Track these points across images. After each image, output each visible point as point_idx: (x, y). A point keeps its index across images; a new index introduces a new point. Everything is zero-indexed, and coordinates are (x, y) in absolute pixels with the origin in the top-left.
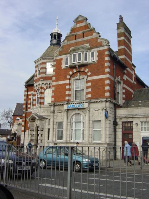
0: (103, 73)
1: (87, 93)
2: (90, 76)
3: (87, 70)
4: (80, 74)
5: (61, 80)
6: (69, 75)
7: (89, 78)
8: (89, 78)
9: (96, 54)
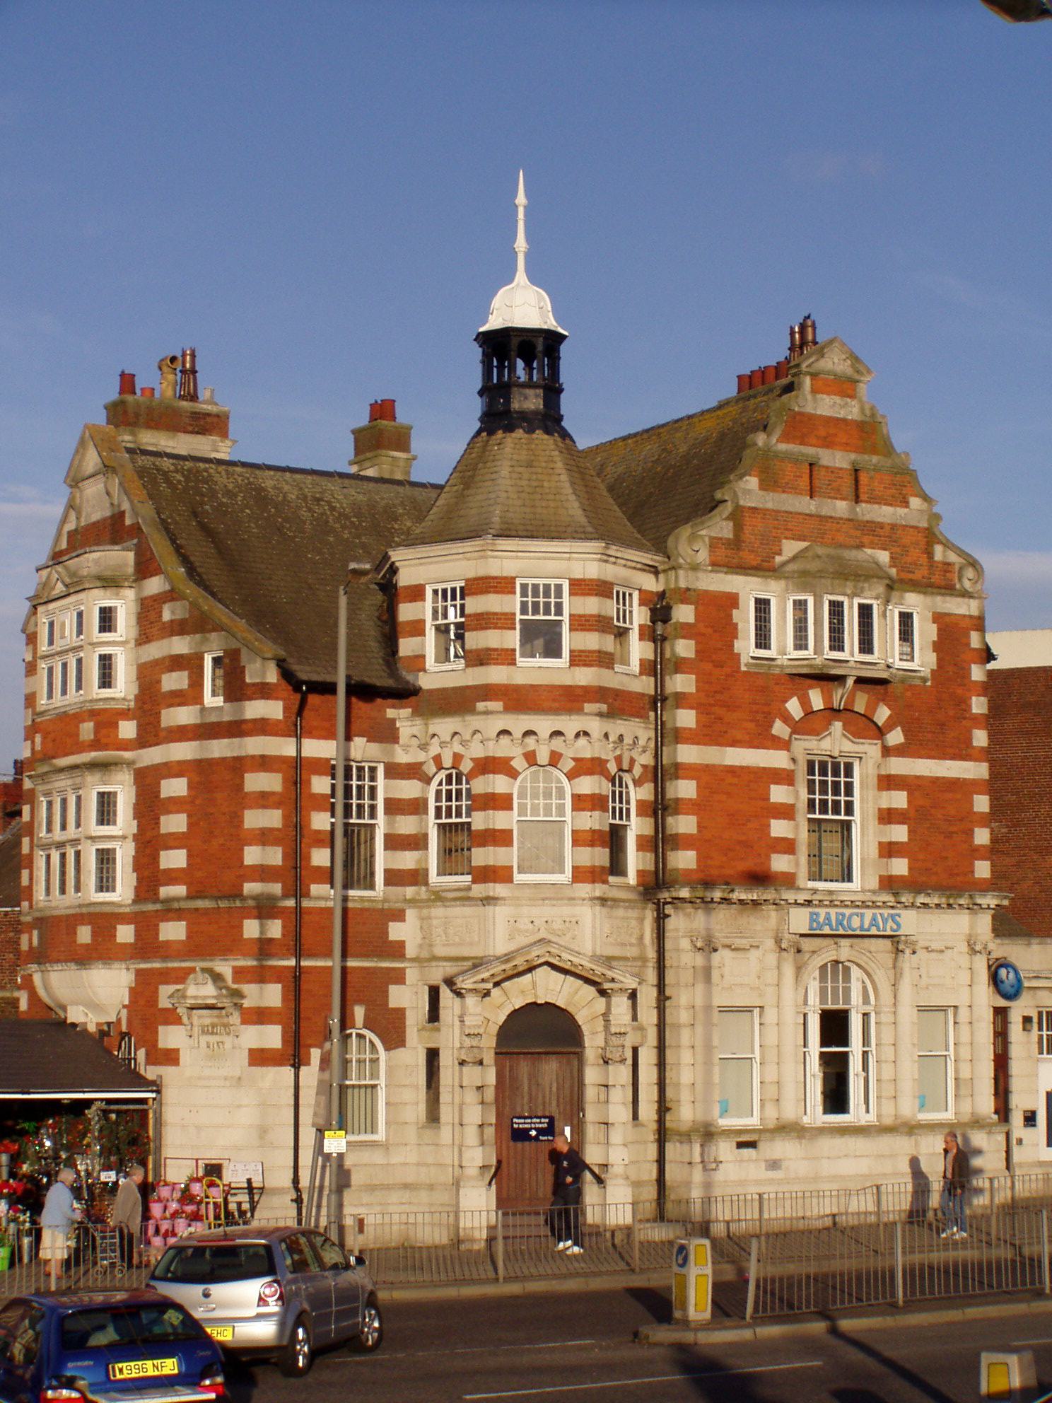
0: (963, 752)
1: (889, 850)
2: (900, 751)
3: (883, 714)
4: (845, 728)
5: (734, 743)
6: (787, 718)
7: (900, 766)
8: (900, 766)
9: (924, 631)
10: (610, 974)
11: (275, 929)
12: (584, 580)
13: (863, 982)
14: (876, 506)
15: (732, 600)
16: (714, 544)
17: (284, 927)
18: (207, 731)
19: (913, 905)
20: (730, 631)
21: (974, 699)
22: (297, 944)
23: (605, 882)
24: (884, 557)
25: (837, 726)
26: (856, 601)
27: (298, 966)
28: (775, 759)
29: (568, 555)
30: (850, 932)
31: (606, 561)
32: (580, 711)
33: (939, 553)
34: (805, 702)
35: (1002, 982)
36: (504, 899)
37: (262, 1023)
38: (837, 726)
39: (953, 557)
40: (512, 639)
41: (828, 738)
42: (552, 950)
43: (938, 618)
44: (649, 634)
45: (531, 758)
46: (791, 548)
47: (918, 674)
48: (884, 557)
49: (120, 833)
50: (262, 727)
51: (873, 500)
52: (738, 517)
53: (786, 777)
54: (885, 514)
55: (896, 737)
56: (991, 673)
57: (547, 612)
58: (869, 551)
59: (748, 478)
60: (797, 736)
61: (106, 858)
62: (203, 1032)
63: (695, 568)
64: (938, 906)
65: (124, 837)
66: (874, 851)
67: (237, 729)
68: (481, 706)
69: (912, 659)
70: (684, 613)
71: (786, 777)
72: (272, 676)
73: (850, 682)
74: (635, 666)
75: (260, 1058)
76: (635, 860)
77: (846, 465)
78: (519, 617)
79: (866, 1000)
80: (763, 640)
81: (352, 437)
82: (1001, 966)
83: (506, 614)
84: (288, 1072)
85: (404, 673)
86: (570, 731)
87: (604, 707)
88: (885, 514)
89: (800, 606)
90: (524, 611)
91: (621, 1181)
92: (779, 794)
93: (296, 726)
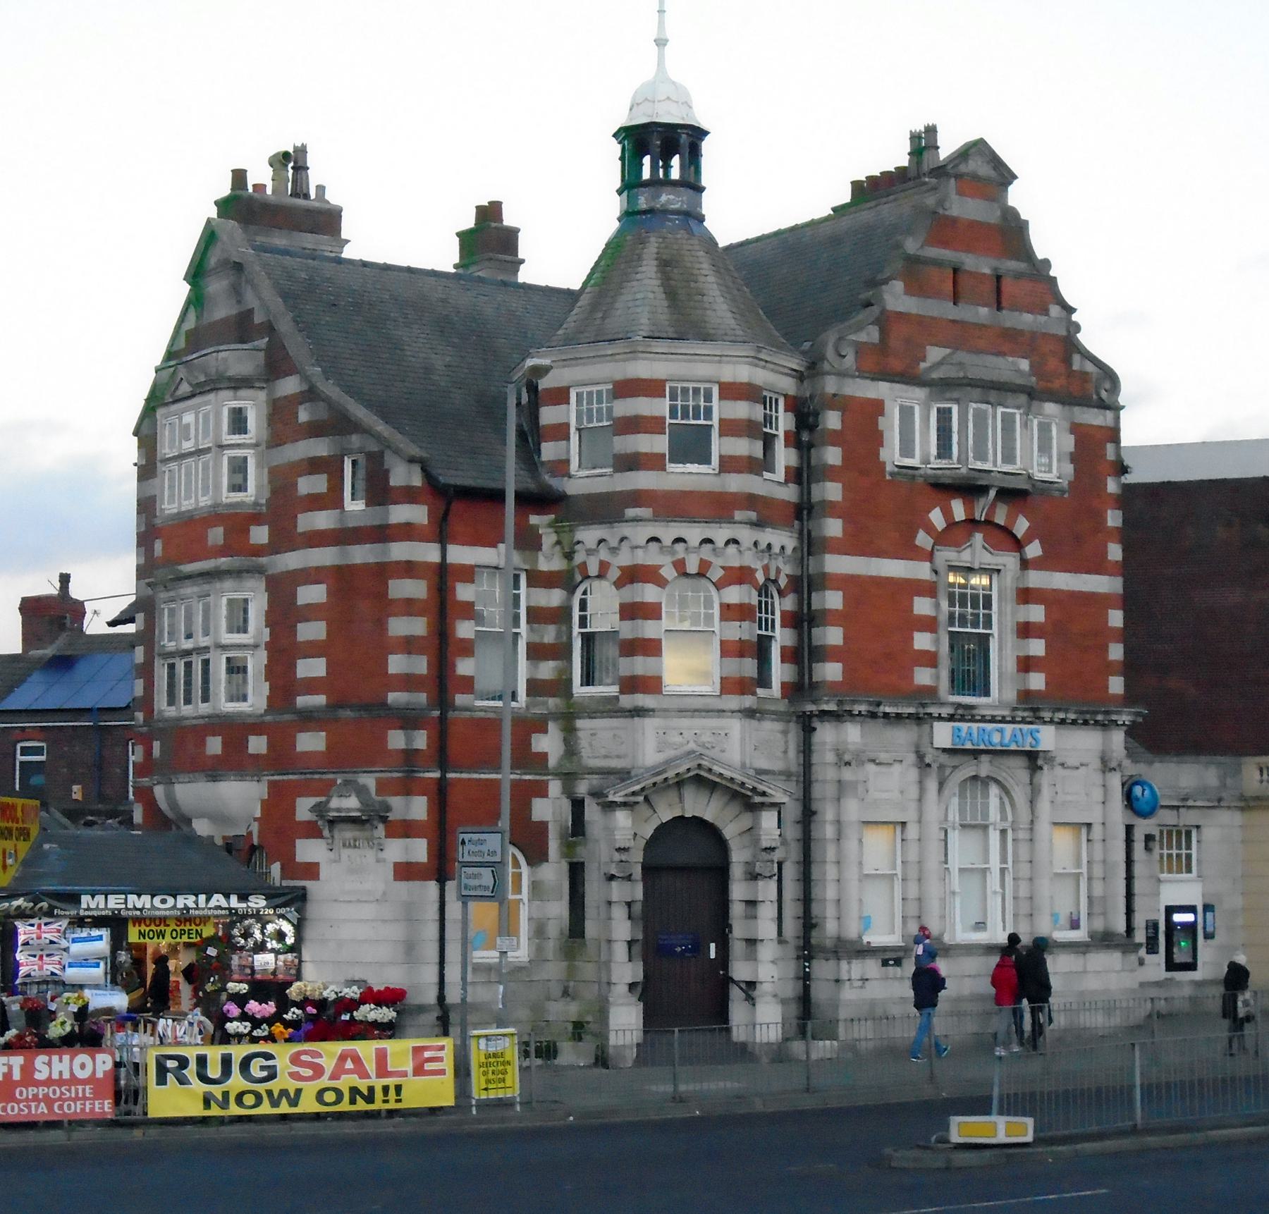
0: (1097, 566)
1: (1026, 665)
2: (1039, 564)
6: (930, 529)
7: (1036, 579)
8: (1036, 579)
9: (1063, 442)
10: (761, 788)
11: (421, 740)
12: (734, 384)
13: (1001, 798)
14: (1017, 313)
15: (877, 408)
16: (860, 349)
17: (428, 738)
18: (343, 536)
19: (1051, 722)
20: (877, 439)
21: (1109, 512)
22: (441, 755)
23: (754, 694)
24: (1024, 365)
25: (978, 538)
26: (1000, 410)
27: (443, 778)
28: (921, 571)
29: (718, 358)
30: (991, 748)
31: (756, 366)
32: (731, 521)
33: (1076, 360)
34: (947, 513)
35: (1138, 799)
36: (653, 710)
37: (408, 836)
38: (978, 538)
39: (1090, 367)
40: (659, 444)
41: (968, 550)
42: (703, 763)
43: (1076, 429)
44: (794, 440)
45: (680, 566)
46: (935, 354)
47: (1056, 485)
48: (1024, 365)
49: (251, 641)
50: (407, 532)
51: (1016, 308)
52: (886, 321)
53: (930, 590)
54: (1027, 320)
55: (1034, 550)
56: (1128, 488)
57: (697, 417)
58: (1010, 359)
59: (894, 282)
60: (939, 548)
61: (236, 669)
62: (344, 845)
63: (842, 374)
64: (1074, 722)
65: (256, 646)
66: (1011, 665)
67: (382, 534)
68: (631, 512)
69: (1050, 471)
70: (832, 420)
71: (930, 590)
72: (417, 480)
73: (992, 493)
74: (780, 475)
75: (405, 871)
76: (779, 672)
77: (987, 271)
78: (668, 421)
79: (1004, 818)
80: (907, 450)
81: (457, 239)
82: (1137, 783)
83: (656, 418)
84: (432, 887)
85: (547, 477)
86: (720, 540)
87: (753, 515)
88: (1027, 320)
89: (944, 416)
90: (673, 414)
91: (769, 998)
92: (922, 606)
93: (441, 533)
